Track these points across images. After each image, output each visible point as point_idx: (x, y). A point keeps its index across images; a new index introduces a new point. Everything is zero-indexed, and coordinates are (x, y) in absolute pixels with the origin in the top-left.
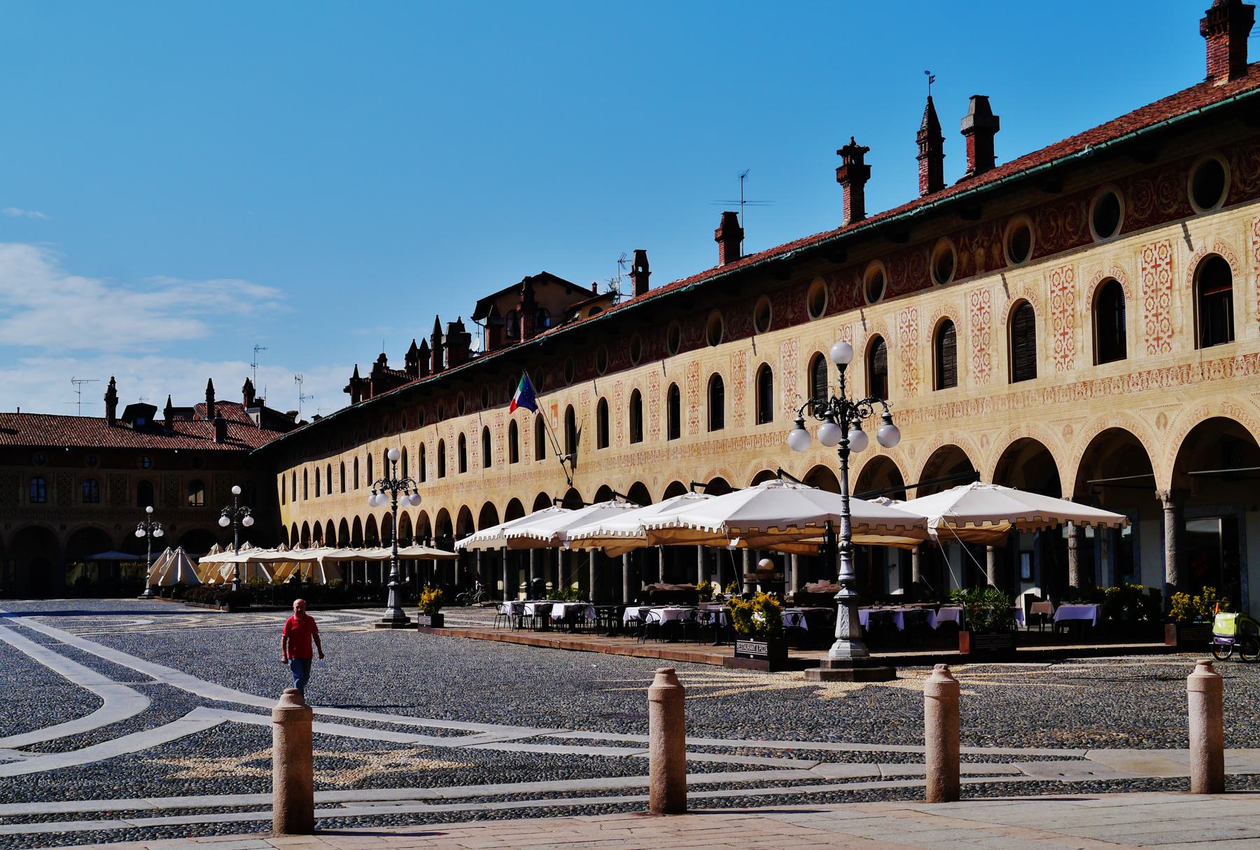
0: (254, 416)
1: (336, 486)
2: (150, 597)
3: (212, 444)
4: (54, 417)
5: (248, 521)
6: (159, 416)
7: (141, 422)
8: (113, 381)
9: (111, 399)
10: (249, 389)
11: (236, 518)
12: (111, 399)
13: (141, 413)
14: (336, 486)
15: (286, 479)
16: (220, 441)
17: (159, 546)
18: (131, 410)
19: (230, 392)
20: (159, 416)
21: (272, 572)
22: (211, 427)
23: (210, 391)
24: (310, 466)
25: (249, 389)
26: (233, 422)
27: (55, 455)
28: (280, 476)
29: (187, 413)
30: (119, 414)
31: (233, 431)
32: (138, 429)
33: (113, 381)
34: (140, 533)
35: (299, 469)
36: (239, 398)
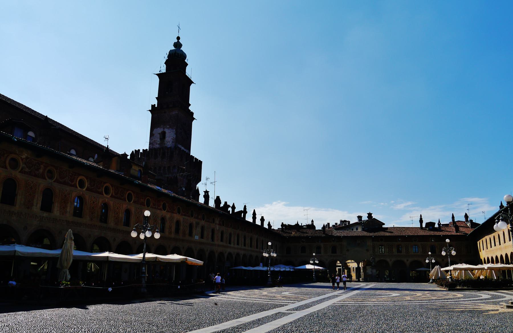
0: (469, 224)
1: (497, 243)
2: (432, 283)
3: (454, 233)
4: (404, 228)
5: (454, 253)
6: (436, 226)
7: (431, 227)
8: (421, 216)
9: (421, 221)
10: (466, 216)
11: (448, 252)
12: (421, 221)
13: (431, 225)
14: (497, 243)
15: (480, 243)
16: (457, 232)
17: (434, 265)
18: (428, 224)
19: (460, 217)
20: (436, 226)
21: (473, 274)
22: (454, 229)
23: (453, 217)
24: (487, 237)
25: (466, 216)
26: (462, 227)
27: (403, 238)
28: (478, 242)
29: (447, 225)
30: (424, 226)
31: (461, 229)
32: (430, 230)
33: (421, 216)
34: (427, 261)
35: (484, 239)
36: (464, 220)
